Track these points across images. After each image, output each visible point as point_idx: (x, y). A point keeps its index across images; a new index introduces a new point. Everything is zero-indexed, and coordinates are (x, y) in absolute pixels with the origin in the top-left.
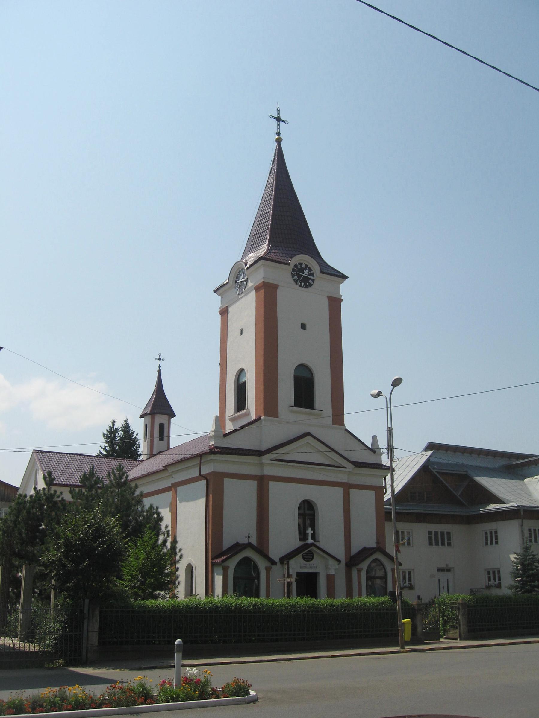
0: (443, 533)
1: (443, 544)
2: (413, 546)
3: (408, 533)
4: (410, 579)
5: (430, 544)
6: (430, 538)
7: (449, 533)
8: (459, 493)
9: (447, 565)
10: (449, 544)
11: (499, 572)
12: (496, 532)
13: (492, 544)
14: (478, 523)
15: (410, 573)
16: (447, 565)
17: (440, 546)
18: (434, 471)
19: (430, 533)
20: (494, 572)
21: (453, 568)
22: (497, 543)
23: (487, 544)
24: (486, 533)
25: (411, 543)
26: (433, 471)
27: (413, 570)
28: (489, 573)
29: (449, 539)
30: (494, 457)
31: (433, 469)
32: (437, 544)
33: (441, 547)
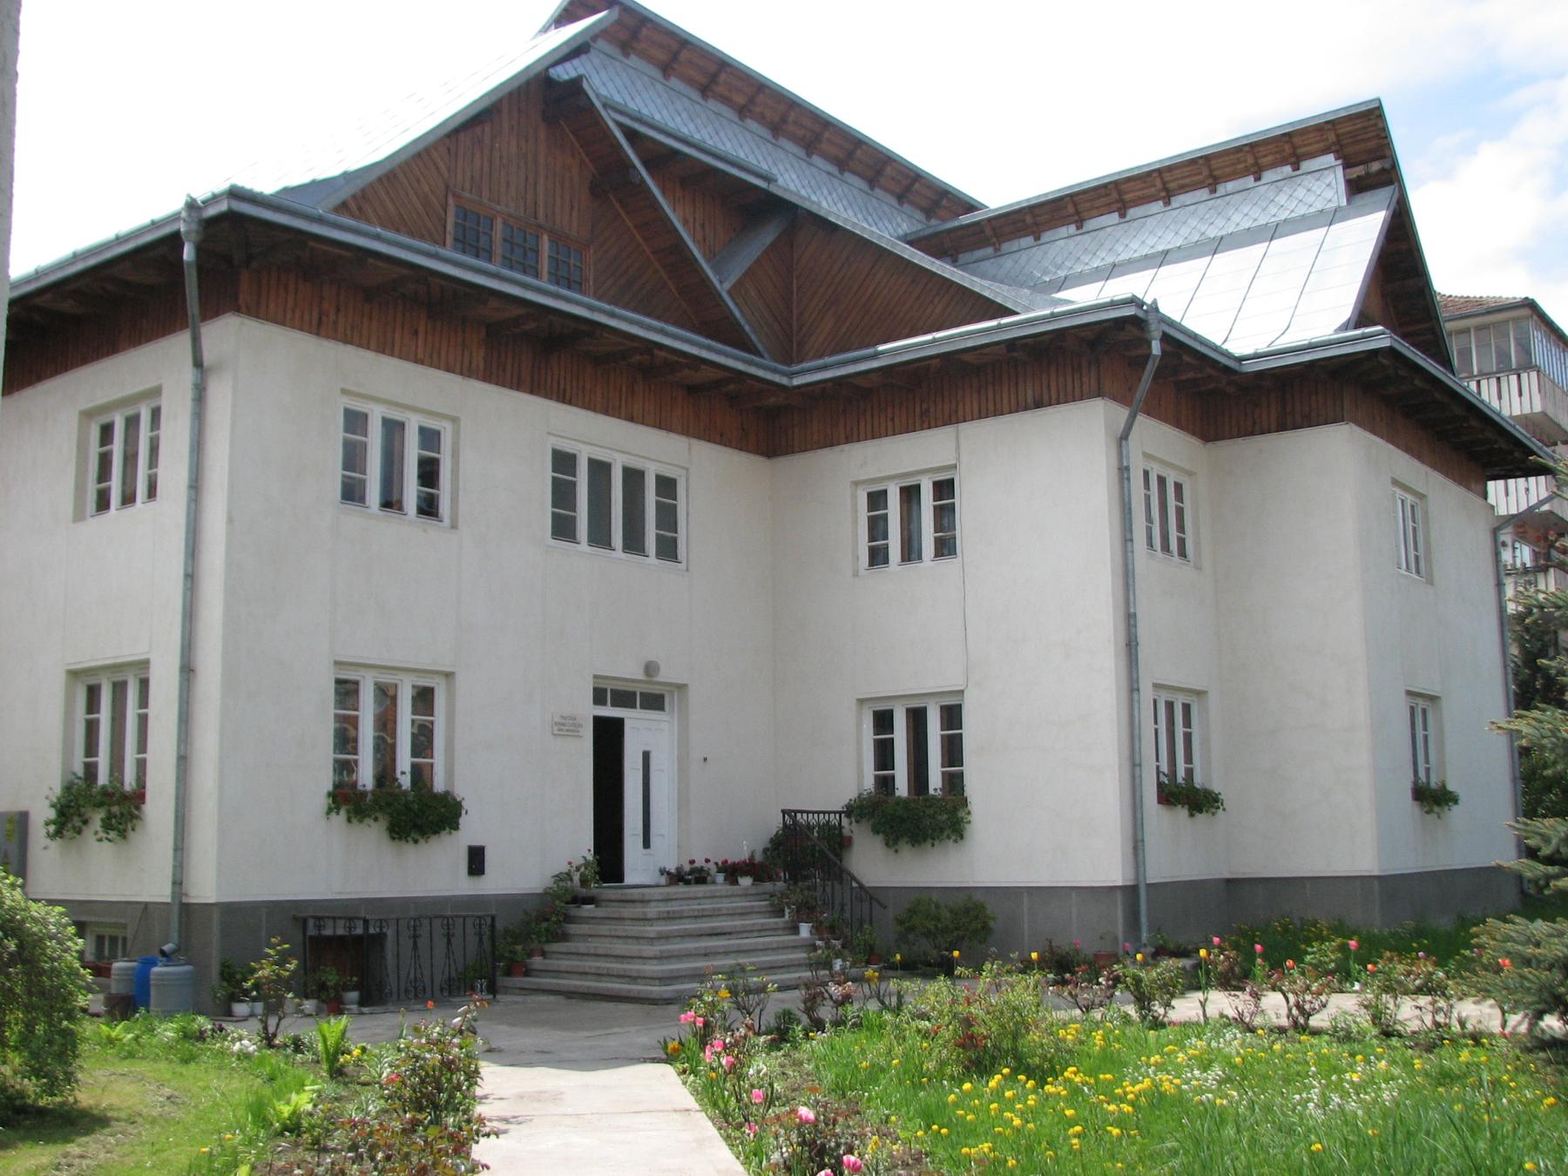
0: (633, 478)
1: (634, 543)
2: (454, 526)
3: (430, 438)
4: (423, 741)
5: (563, 529)
6: (563, 494)
7: (667, 486)
8: (733, 279)
9: (650, 669)
10: (668, 550)
11: (952, 716)
12: (944, 489)
13: (910, 552)
14: (830, 442)
15: (424, 698)
16: (650, 669)
17: (619, 553)
18: (609, 118)
19: (564, 462)
20: (917, 718)
21: (682, 687)
22: (945, 547)
23: (878, 557)
24: (877, 499)
25: (445, 507)
26: (603, 113)
27: (449, 675)
28: (883, 721)
29: (668, 517)
30: (872, 183)
31: (605, 106)
32: (600, 537)
33: (624, 556)
